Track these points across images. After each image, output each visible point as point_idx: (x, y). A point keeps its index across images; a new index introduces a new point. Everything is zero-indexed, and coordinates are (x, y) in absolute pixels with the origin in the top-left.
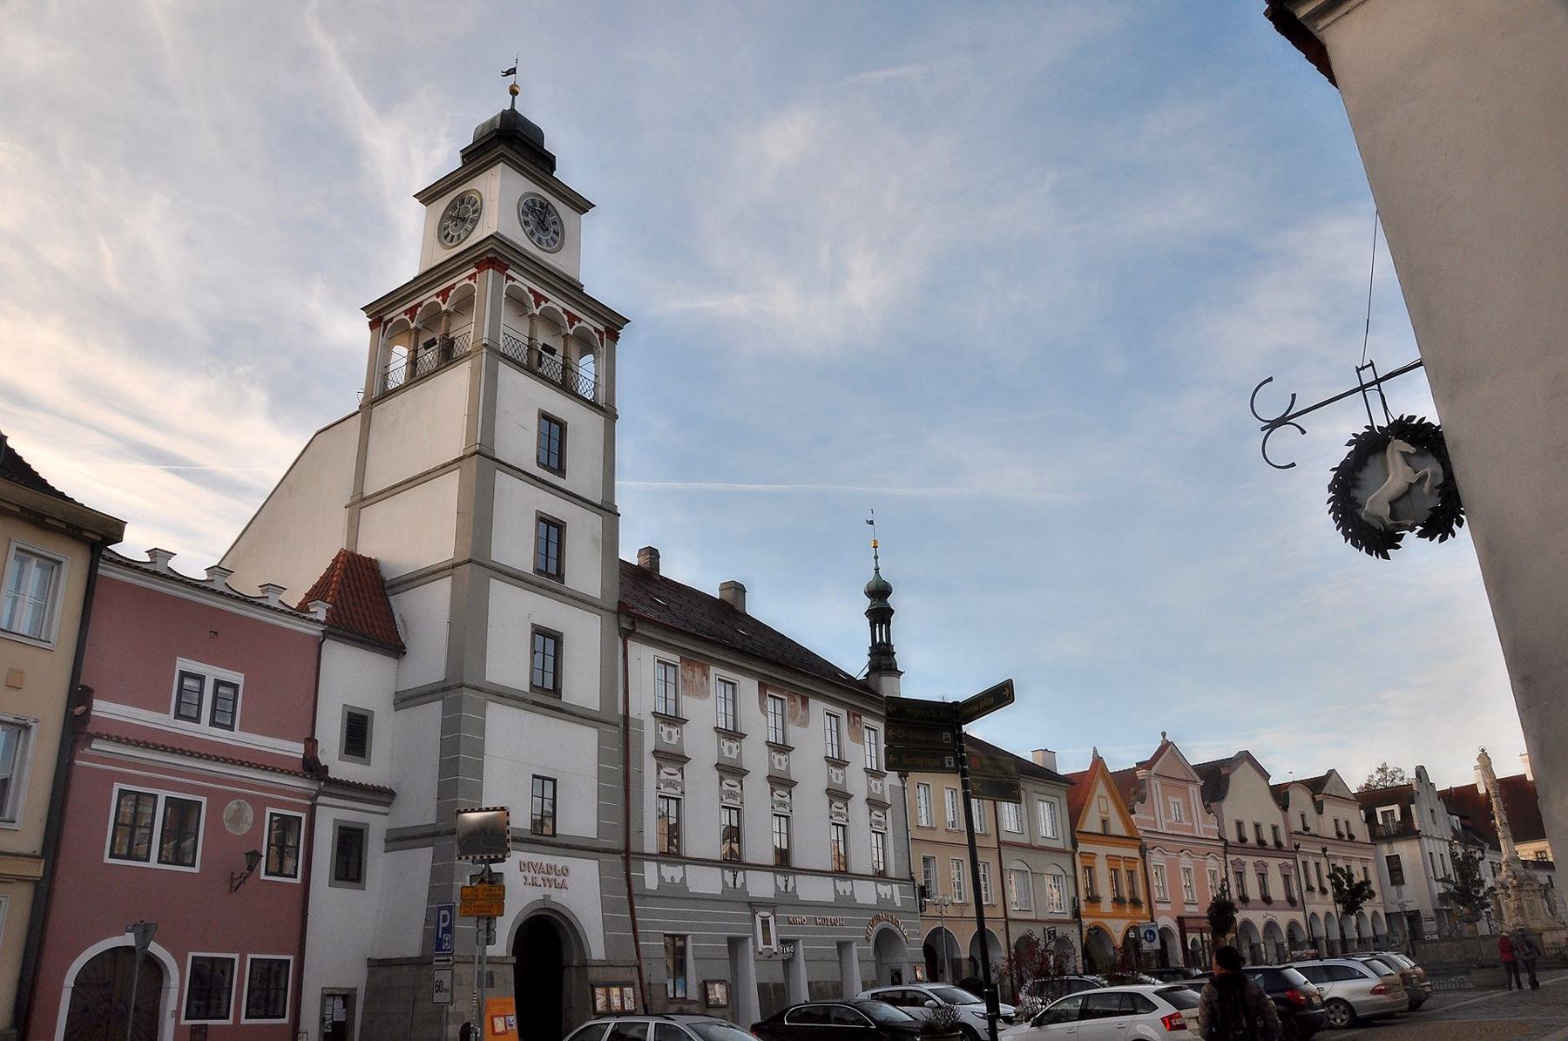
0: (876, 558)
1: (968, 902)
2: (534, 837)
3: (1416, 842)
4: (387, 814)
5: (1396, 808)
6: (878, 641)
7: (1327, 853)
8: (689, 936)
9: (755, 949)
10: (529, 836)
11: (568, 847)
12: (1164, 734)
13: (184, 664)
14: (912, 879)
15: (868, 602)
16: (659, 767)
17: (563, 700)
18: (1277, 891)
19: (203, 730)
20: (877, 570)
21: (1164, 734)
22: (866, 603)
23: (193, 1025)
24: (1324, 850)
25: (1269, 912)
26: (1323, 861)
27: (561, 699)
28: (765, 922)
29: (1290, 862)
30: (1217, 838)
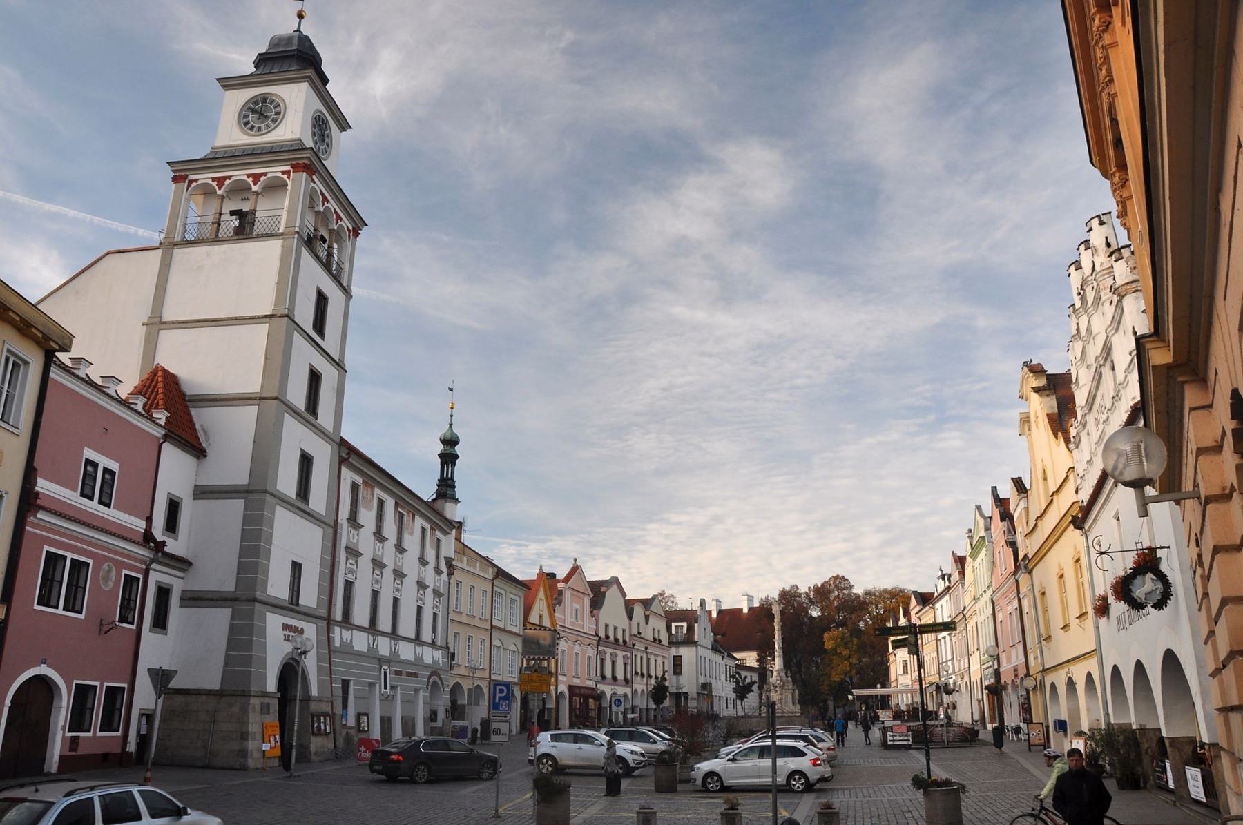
0: (451, 416)
1: (460, 664)
2: (290, 606)
3: (694, 648)
4: (182, 578)
5: (685, 624)
6: (445, 476)
7: (648, 650)
8: (352, 682)
9: (380, 691)
10: (286, 605)
11: (304, 614)
12: (575, 560)
13: (89, 454)
14: (448, 648)
16: (347, 559)
17: (310, 506)
18: (620, 675)
19: (93, 506)
20: (451, 425)
21: (575, 560)
22: (440, 448)
23: (72, 737)
24: (646, 648)
25: (616, 687)
26: (645, 656)
27: (308, 505)
28: (385, 673)
29: (629, 654)
30: (594, 634)
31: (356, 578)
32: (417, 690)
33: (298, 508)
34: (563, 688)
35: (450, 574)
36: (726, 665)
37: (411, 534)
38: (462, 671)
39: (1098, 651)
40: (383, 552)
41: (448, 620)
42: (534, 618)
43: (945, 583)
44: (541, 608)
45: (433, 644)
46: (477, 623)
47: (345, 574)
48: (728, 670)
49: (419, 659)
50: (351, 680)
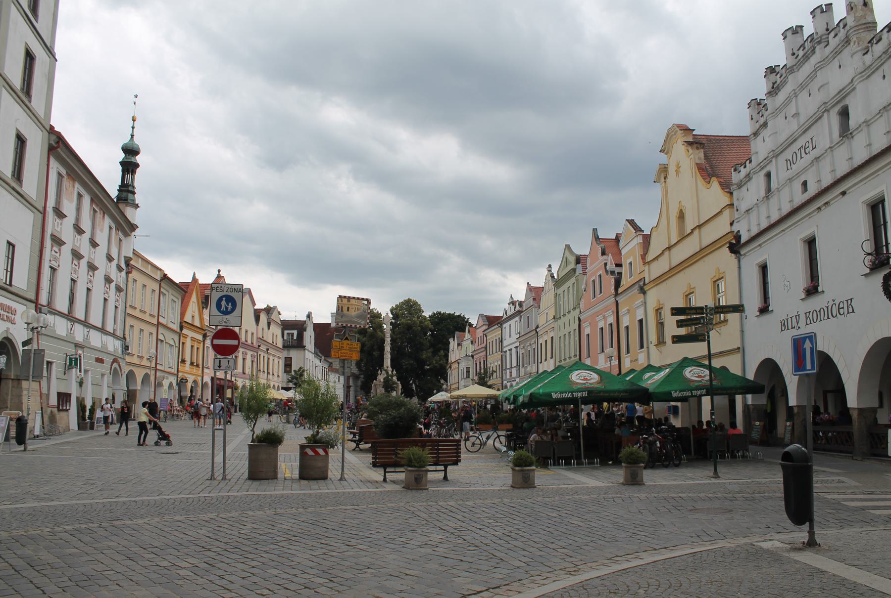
0: (133, 128)
3: (302, 352)
8: (54, 363)
9: (76, 374)
12: (219, 271)
14: (124, 338)
15: (122, 156)
16: (52, 246)
18: (248, 371)
20: (132, 136)
21: (219, 271)
24: (268, 350)
29: (255, 354)
31: (59, 266)
32: (103, 375)
33: (14, 189)
34: (207, 379)
35: (128, 273)
36: (322, 367)
37: (102, 231)
38: (135, 360)
39: (741, 349)
40: (80, 244)
41: (126, 315)
42: (188, 318)
43: (515, 307)
44: (194, 310)
45: (113, 335)
46: (147, 317)
47: (50, 261)
48: (323, 371)
49: (104, 346)
50: (53, 362)
